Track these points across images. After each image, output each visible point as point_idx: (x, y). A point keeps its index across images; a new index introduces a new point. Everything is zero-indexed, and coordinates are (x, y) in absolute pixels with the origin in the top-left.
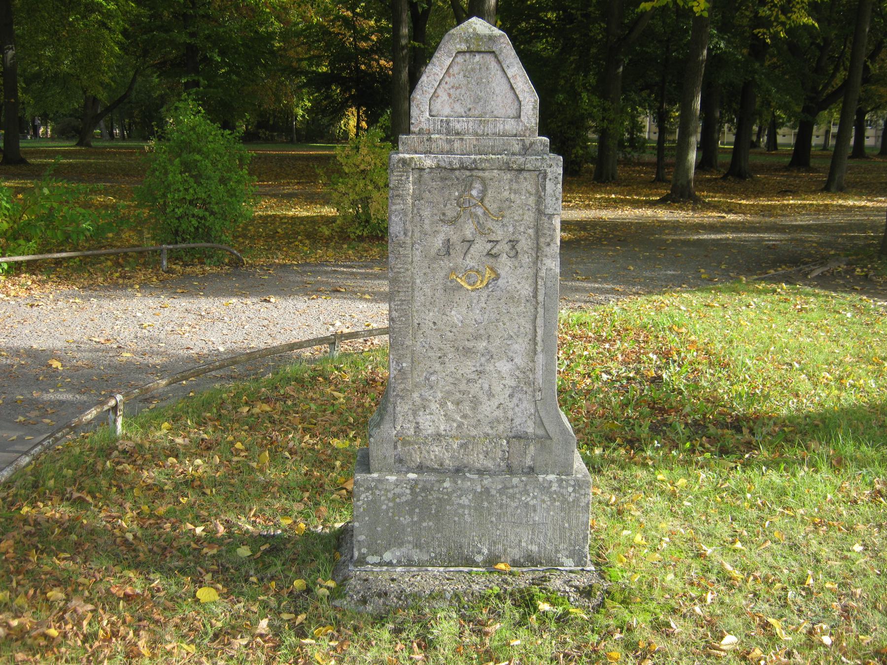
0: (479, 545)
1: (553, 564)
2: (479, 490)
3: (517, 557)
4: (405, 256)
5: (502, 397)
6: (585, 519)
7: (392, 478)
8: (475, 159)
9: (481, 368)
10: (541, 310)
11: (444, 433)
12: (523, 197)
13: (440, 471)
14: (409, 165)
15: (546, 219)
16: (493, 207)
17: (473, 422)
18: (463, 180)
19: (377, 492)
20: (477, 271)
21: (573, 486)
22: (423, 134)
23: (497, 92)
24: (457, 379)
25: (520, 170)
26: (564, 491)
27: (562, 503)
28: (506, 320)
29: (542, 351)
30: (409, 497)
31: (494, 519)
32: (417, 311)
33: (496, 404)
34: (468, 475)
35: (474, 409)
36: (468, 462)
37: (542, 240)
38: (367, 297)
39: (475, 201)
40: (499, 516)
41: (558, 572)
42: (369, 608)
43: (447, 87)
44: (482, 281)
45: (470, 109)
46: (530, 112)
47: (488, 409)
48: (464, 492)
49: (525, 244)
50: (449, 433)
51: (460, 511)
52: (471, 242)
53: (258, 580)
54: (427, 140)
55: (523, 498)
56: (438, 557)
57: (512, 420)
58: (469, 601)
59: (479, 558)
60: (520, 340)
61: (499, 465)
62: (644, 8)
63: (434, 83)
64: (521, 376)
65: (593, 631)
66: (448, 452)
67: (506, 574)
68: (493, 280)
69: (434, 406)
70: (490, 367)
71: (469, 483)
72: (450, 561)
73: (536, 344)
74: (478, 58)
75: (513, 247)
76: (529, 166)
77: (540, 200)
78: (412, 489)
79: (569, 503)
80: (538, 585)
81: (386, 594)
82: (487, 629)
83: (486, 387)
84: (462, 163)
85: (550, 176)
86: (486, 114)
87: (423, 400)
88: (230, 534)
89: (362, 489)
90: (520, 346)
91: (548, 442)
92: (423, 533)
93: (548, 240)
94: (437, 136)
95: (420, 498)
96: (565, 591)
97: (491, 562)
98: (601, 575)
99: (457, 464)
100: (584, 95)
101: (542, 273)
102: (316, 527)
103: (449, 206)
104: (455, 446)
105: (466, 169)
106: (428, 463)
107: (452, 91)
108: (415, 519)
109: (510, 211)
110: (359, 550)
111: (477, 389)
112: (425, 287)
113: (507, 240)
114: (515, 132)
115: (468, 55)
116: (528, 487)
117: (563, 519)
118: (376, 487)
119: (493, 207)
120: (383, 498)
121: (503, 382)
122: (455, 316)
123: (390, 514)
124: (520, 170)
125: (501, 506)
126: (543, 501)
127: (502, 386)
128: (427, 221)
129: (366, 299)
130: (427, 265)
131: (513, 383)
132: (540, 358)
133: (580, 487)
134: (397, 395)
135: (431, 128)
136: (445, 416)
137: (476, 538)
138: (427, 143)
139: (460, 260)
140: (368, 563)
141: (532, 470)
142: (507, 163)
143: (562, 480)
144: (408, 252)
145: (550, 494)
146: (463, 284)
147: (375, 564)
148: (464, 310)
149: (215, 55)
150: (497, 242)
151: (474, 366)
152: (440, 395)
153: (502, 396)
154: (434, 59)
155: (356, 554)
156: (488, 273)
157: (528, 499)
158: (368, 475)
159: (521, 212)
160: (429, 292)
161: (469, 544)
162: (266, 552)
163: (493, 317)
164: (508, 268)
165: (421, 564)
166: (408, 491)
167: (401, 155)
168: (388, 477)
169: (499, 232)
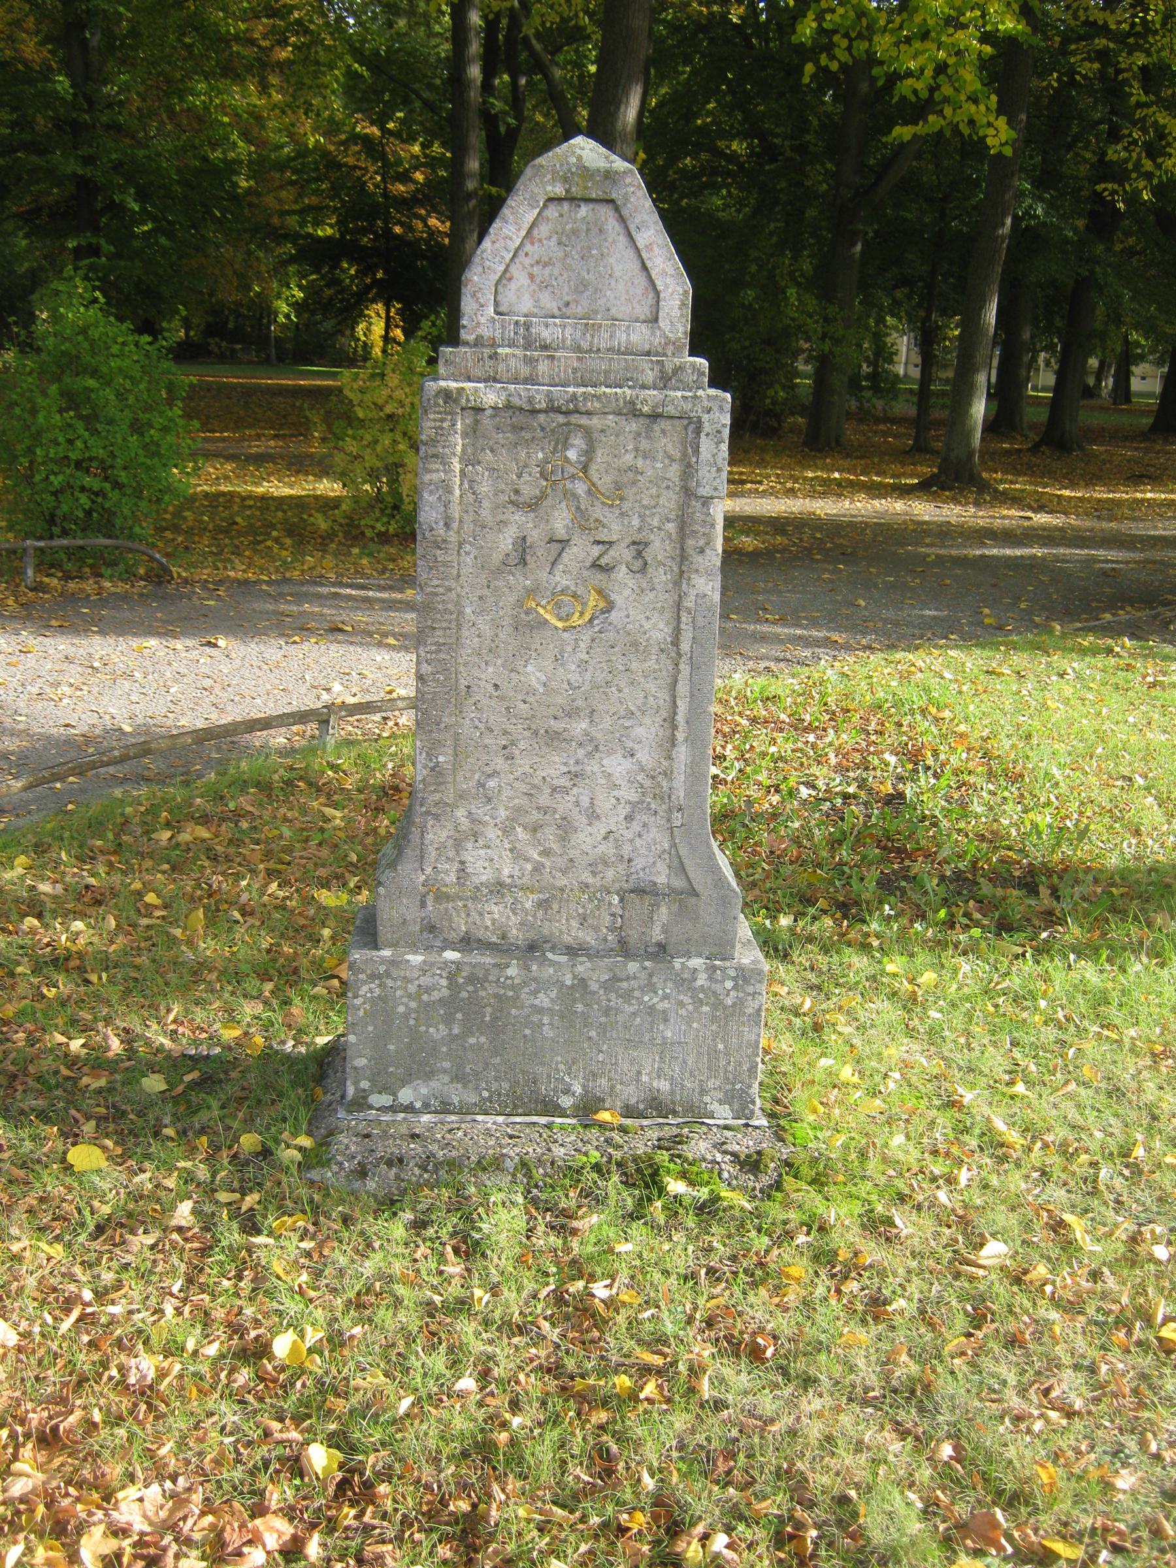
0: (567, 1079)
1: (696, 1114)
2: (569, 983)
3: (633, 1101)
4: (445, 564)
5: (613, 820)
6: (753, 1037)
7: (416, 959)
8: (574, 394)
9: (578, 768)
10: (685, 668)
11: (508, 881)
12: (659, 465)
13: (502, 947)
14: (456, 401)
15: (699, 504)
16: (605, 481)
17: (561, 862)
18: (553, 431)
19: (390, 983)
21: (734, 979)
22: (483, 346)
23: (617, 274)
24: (534, 786)
25: (655, 416)
26: (717, 987)
27: (715, 1007)
28: (623, 684)
29: (686, 740)
30: (445, 992)
31: (593, 1034)
32: (466, 664)
33: (603, 832)
34: (550, 955)
35: (564, 839)
36: (552, 934)
37: (690, 542)
38: (391, 641)
39: (572, 470)
40: (603, 1030)
41: (704, 1129)
42: (371, 1184)
43: (528, 261)
44: (582, 614)
45: (567, 304)
46: (676, 313)
47: (588, 839)
48: (541, 986)
49: (660, 548)
50: (519, 882)
51: (535, 1018)
52: (564, 543)
53: (178, 1133)
54: (490, 357)
55: (646, 998)
56: (495, 1098)
57: (630, 861)
58: (546, 1175)
59: (566, 1102)
60: (647, 720)
61: (605, 940)
62: (900, 136)
63: (504, 253)
64: (648, 783)
65: (759, 1231)
66: (516, 914)
67: (612, 1129)
68: (603, 612)
69: (492, 834)
70: (592, 767)
71: (551, 970)
72: (515, 1106)
73: (674, 727)
74: (584, 210)
76: (670, 410)
77: (688, 471)
78: (451, 978)
79: (725, 1008)
80: (668, 1150)
81: (401, 1160)
82: (575, 1224)
83: (585, 801)
84: (551, 400)
85: (707, 427)
86: (595, 312)
87: (473, 821)
88: (131, 1052)
89: (362, 976)
90: (647, 731)
91: (693, 900)
92: (470, 1055)
93: (701, 543)
94: (507, 350)
95: (464, 994)
96: (714, 1162)
97: (587, 1109)
98: (779, 1134)
99: (531, 935)
100: (792, 292)
101: (689, 603)
102: (283, 1042)
103: (526, 477)
104: (528, 905)
105: (558, 410)
106: (481, 934)
107: (536, 270)
108: (456, 1031)
109: (634, 490)
110: (356, 1083)
111: (570, 805)
113: (628, 540)
114: (647, 347)
115: (566, 205)
116: (655, 979)
117: (715, 1036)
118: (388, 974)
119: (605, 481)
120: (399, 993)
121: (616, 793)
122: (534, 674)
123: (412, 1022)
124: (655, 416)
125: (607, 1011)
126: (681, 1004)
127: (613, 801)
128: (486, 504)
129: (389, 645)
130: (485, 582)
131: (633, 796)
132: (682, 753)
133: (746, 980)
134: (428, 813)
135: (498, 335)
136: (511, 850)
137: (562, 1067)
139: (543, 575)
140: (371, 1107)
141: (661, 952)
143: (714, 968)
144: (452, 557)
145: (693, 992)
146: (548, 617)
147: (383, 1109)
148: (549, 664)
149: (130, 200)
150: (611, 543)
151: (565, 764)
152: (503, 813)
153: (614, 820)
154: (505, 211)
155: (351, 1091)
156: (593, 600)
157: (655, 1000)
158: (374, 953)
160: (487, 630)
161: (549, 1076)
162: (193, 1085)
163: (601, 677)
164: (627, 592)
165: (464, 1111)
166: (444, 982)
167: (443, 384)
168: (409, 957)
169: (616, 527)
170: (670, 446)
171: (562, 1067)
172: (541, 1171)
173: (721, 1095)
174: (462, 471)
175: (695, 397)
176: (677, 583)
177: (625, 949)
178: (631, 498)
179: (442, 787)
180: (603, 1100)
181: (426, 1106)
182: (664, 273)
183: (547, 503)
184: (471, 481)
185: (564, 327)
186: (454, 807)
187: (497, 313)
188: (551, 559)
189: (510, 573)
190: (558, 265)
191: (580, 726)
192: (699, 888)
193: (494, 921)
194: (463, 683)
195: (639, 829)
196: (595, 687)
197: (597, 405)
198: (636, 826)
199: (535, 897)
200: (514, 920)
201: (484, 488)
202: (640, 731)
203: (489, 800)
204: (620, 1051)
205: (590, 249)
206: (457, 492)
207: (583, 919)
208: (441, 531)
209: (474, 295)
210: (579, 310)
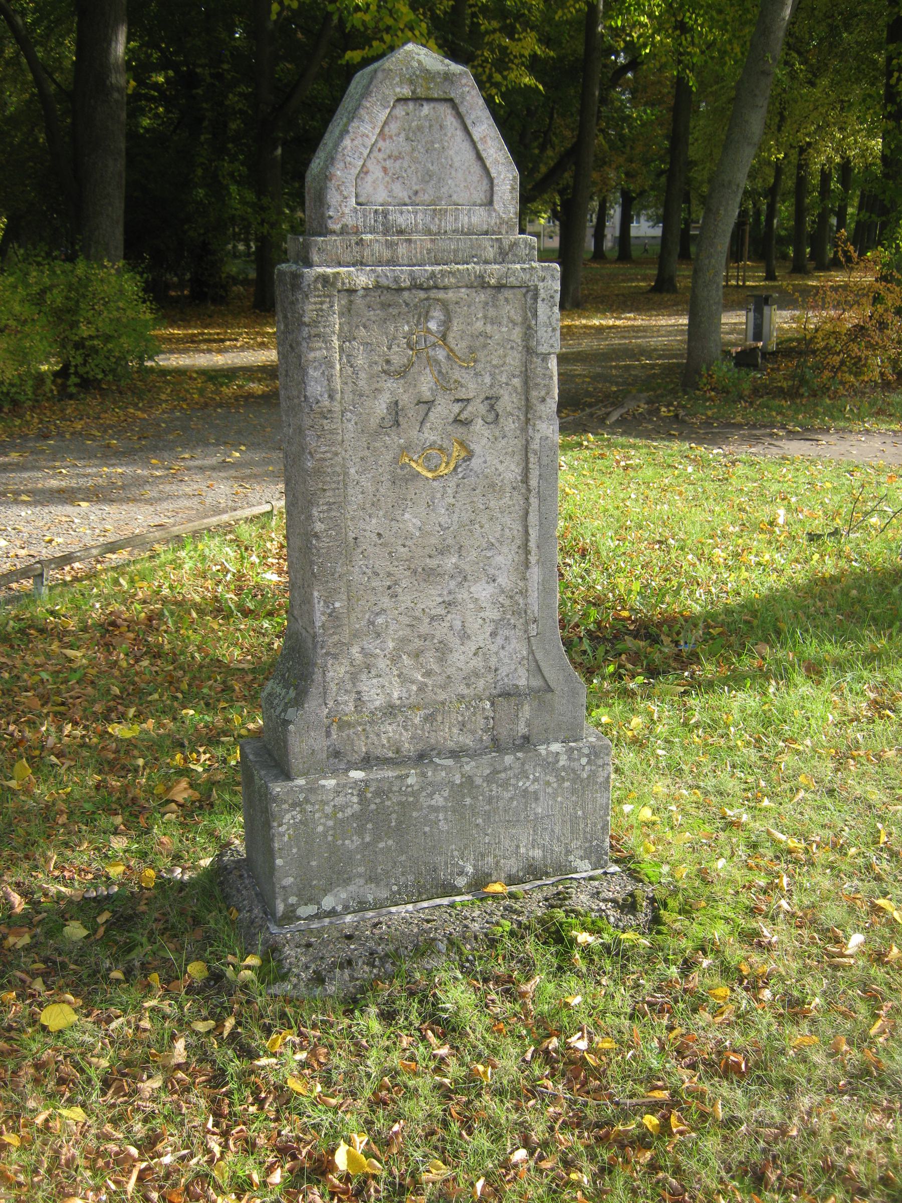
0: (461, 863)
2: (458, 782)
4: (331, 432)
5: (481, 638)
6: (605, 801)
8: (433, 272)
9: (451, 597)
10: (534, 501)
11: (398, 702)
12: (504, 329)
14: (333, 285)
15: (539, 361)
16: (460, 347)
17: (440, 680)
18: (415, 306)
19: (309, 808)
20: (441, 449)
21: (588, 756)
22: (348, 233)
23: (457, 164)
25: (500, 287)
26: (575, 765)
27: (574, 782)
28: (484, 521)
31: (480, 821)
33: (473, 649)
34: (436, 760)
35: (442, 660)
36: (437, 742)
37: (534, 393)
38: (24, 498)
39: (432, 339)
40: (487, 816)
41: (575, 884)
43: (381, 156)
45: (416, 193)
46: (508, 196)
47: (462, 657)
48: (436, 787)
49: (508, 401)
50: (406, 702)
51: (432, 817)
52: (430, 404)
53: (124, 974)
54: (357, 244)
56: (403, 890)
57: (496, 670)
58: (473, 949)
59: (461, 882)
60: (505, 550)
61: (481, 740)
62: (352, 58)
63: (362, 149)
64: (507, 602)
65: (666, 960)
66: (407, 730)
67: (504, 898)
68: (464, 460)
70: (462, 595)
71: (443, 774)
72: (420, 894)
73: (527, 552)
74: (426, 109)
75: (492, 407)
76: (512, 280)
77: (529, 332)
78: (361, 795)
80: (560, 907)
81: (350, 962)
83: (458, 624)
85: (542, 294)
88: (35, 904)
89: (285, 806)
91: (549, 696)
93: (543, 393)
95: (373, 807)
96: (600, 910)
97: (478, 884)
98: (634, 875)
100: (233, 188)
101: (535, 445)
102: (171, 871)
103: (395, 348)
104: (417, 720)
105: (421, 288)
106: (379, 752)
107: (388, 164)
108: (368, 839)
109: (486, 352)
110: (285, 900)
111: (445, 630)
112: (363, 479)
113: (482, 396)
114: (485, 227)
115: (411, 105)
116: (527, 767)
117: (575, 804)
118: (307, 801)
119: (460, 347)
120: (317, 815)
121: (482, 614)
122: (411, 520)
123: (330, 838)
124: (500, 287)
126: (548, 784)
127: (480, 621)
128: (362, 375)
129: (24, 502)
130: (365, 445)
131: (495, 615)
132: (535, 574)
133: (597, 755)
134: (327, 654)
135: (360, 224)
136: (399, 676)
137: (456, 853)
138: (356, 249)
139: (414, 433)
140: (299, 918)
141: (526, 742)
142: (481, 277)
143: (572, 749)
146: (419, 469)
147: (310, 918)
148: (422, 509)
150: (468, 400)
151: (440, 595)
152: (391, 645)
153: (481, 638)
155: (280, 908)
156: (456, 450)
157: (528, 784)
158: (291, 784)
159: (501, 352)
160: (370, 487)
161: (446, 863)
162: (109, 925)
163: (466, 516)
164: (485, 440)
165: (378, 905)
166: (355, 799)
167: (320, 270)
168: (323, 782)
169: (472, 386)
170: (512, 312)
171: (456, 853)
173: (581, 853)
174: (341, 347)
175: (532, 268)
176: (524, 430)
177: (497, 745)
180: (491, 875)
181: (346, 908)
182: (496, 162)
185: (416, 213)
186: (349, 645)
187: (358, 204)
188: (420, 419)
190: (407, 158)
193: (389, 739)
194: (352, 535)
197: (453, 280)
198: (499, 640)
199: (422, 713)
200: (406, 735)
202: (499, 559)
203: (378, 635)
205: (433, 143)
206: (338, 367)
209: (338, 188)
210: (426, 198)
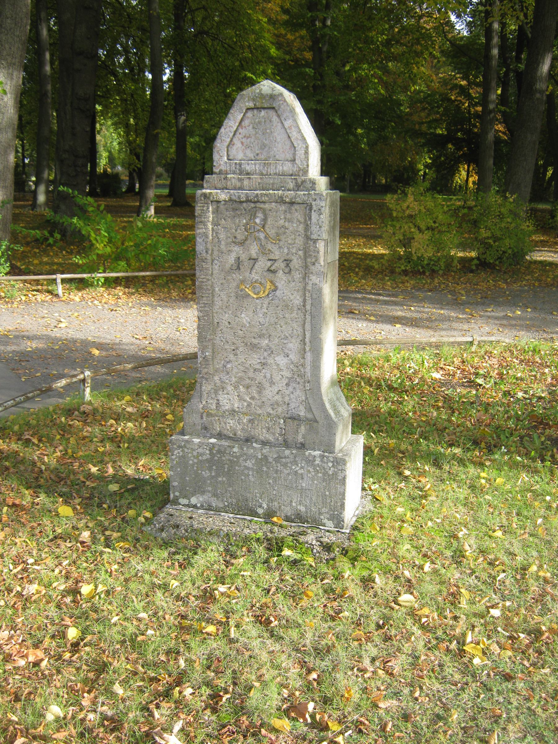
0: (260, 500)
1: (316, 523)
2: (260, 457)
3: (289, 514)
4: (206, 269)
5: (280, 385)
6: (342, 491)
7: (196, 440)
9: (265, 361)
10: (308, 317)
11: (237, 409)
12: (295, 225)
13: (234, 439)
14: (209, 198)
15: (312, 243)
16: (272, 232)
17: (259, 403)
18: (249, 210)
19: (186, 450)
20: (261, 283)
21: (332, 462)
23: (278, 140)
24: (247, 368)
25: (292, 203)
27: (324, 474)
29: (310, 350)
30: (208, 456)
31: (271, 481)
32: (217, 313)
33: (276, 390)
34: (254, 445)
37: (309, 260)
38: (372, 318)
39: (258, 228)
40: (275, 480)
41: (318, 530)
42: (164, 535)
43: (240, 136)
44: (264, 292)
45: (258, 155)
47: (270, 393)
49: (296, 263)
50: (241, 410)
51: (246, 472)
52: (255, 260)
55: (293, 467)
57: (288, 404)
58: (236, 540)
59: (260, 511)
60: (293, 340)
61: (278, 439)
63: (229, 133)
69: (230, 388)
71: (252, 451)
72: (239, 511)
73: (305, 344)
74: (263, 113)
75: (288, 265)
76: (298, 200)
78: (210, 450)
79: (329, 475)
81: (178, 526)
82: (233, 561)
83: (268, 376)
84: (248, 197)
85: (314, 208)
86: (269, 157)
87: (222, 382)
89: (175, 446)
90: (294, 345)
91: (315, 424)
92: (219, 485)
93: (313, 260)
94: (232, 176)
95: (216, 458)
97: (269, 515)
99: (246, 435)
101: (309, 287)
103: (239, 231)
104: (245, 421)
105: (251, 201)
106: (225, 432)
107: (244, 140)
108: (213, 474)
109: (285, 236)
110: (174, 493)
111: (262, 377)
112: (222, 294)
113: (283, 259)
114: (291, 172)
115: (255, 111)
116: (297, 459)
117: (325, 488)
118: (185, 447)
119: (272, 232)
120: (190, 455)
122: (245, 318)
123: (195, 468)
124: (292, 203)
125: (276, 472)
126: (309, 471)
127: (280, 376)
128: (223, 243)
134: (203, 377)
136: (238, 396)
137: (258, 495)
138: (223, 181)
139: (247, 274)
140: (180, 504)
141: (303, 446)
142: (281, 197)
144: (209, 266)
145: (314, 467)
146: (250, 293)
148: (251, 313)
149: (337, 119)
150: (275, 260)
152: (234, 379)
153: (281, 385)
154: (230, 115)
155: (172, 496)
156: (268, 285)
157: (297, 469)
159: (293, 237)
160: (225, 299)
161: (252, 499)
163: (273, 320)
164: (283, 282)
165: (218, 510)
166: (208, 452)
167: (204, 191)
168: (194, 440)
169: (277, 253)
170: (299, 216)
171: (258, 495)
172: (234, 538)
173: (328, 516)
174: (212, 228)
175: (309, 194)
176: (304, 278)
177: (286, 444)
178: (283, 240)
179: (207, 366)
180: (276, 512)
181: (202, 506)
182: (297, 139)
183: (248, 242)
184: (217, 233)
185: (255, 164)
186: (213, 375)
187: (228, 159)
188: (250, 267)
189: (233, 273)
190: (253, 137)
191: (265, 342)
192: (318, 419)
193: (231, 427)
194: (216, 321)
195: (291, 390)
196: (271, 325)
197: (267, 199)
198: (291, 389)
199: (248, 417)
200: (239, 427)
201: (222, 236)
202: (291, 345)
203: (228, 373)
204: (283, 490)
205: (266, 129)
206: (211, 238)
207: (268, 429)
208: (204, 254)
209: (218, 152)
210: (263, 157)
